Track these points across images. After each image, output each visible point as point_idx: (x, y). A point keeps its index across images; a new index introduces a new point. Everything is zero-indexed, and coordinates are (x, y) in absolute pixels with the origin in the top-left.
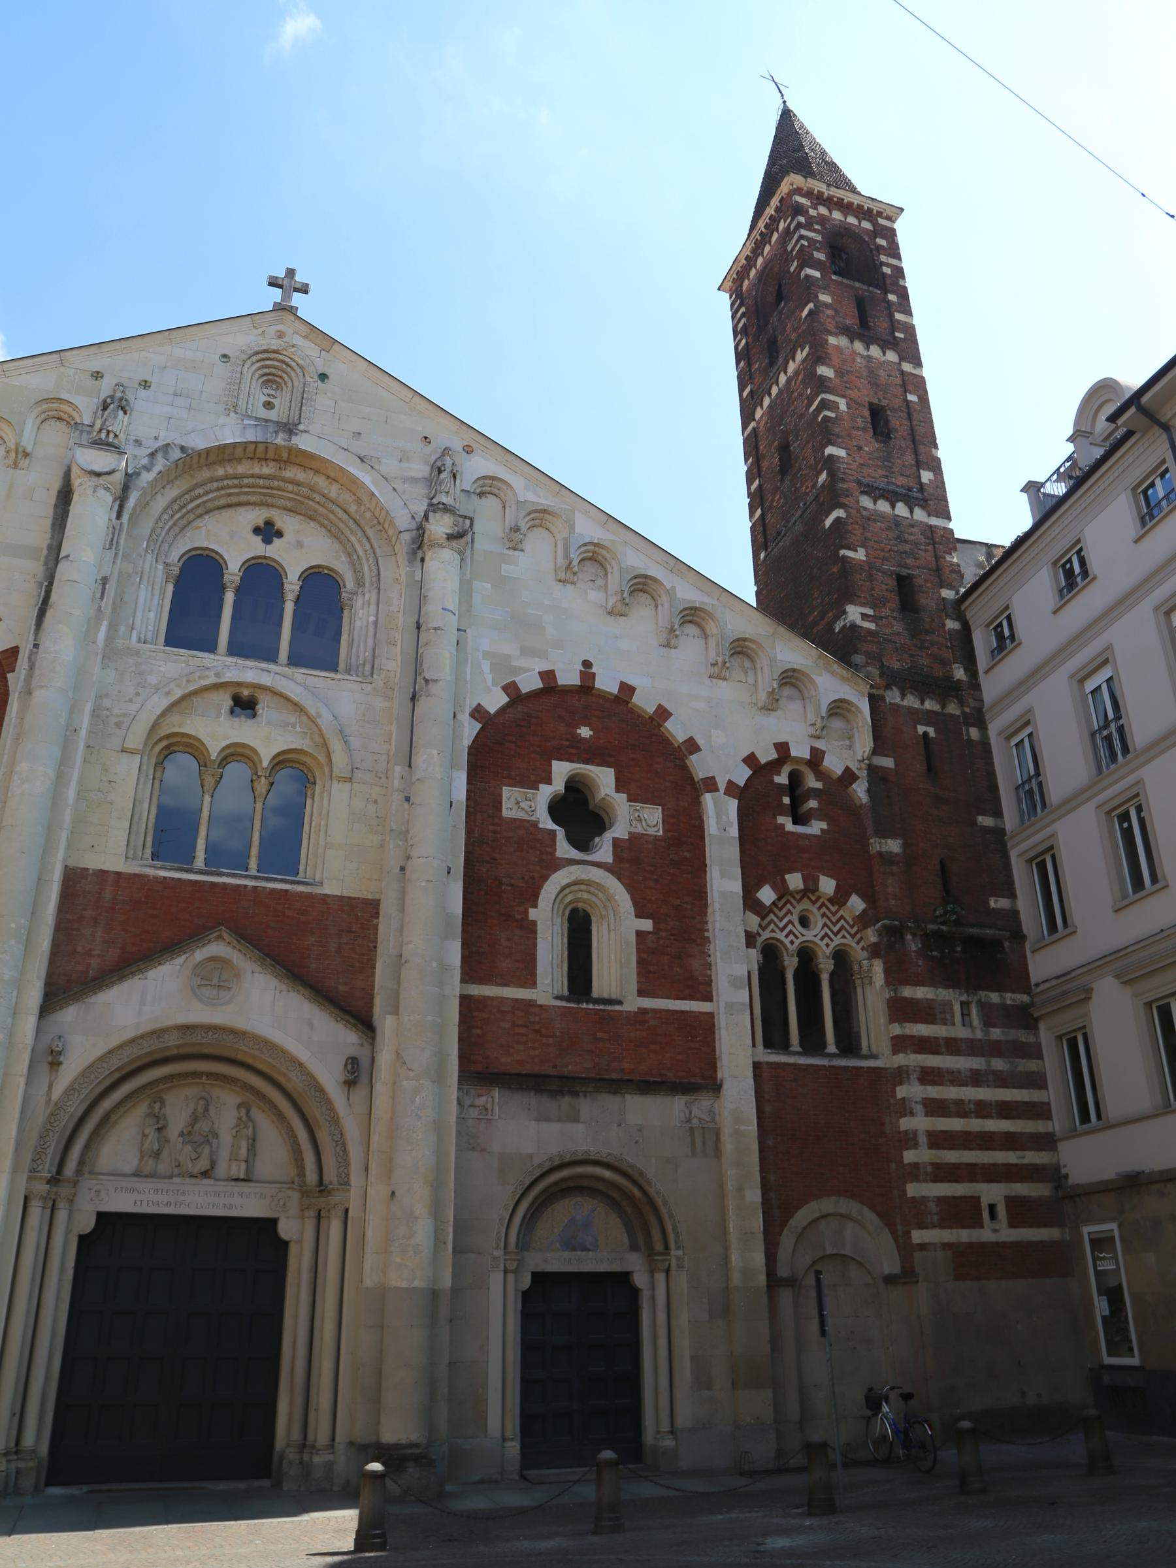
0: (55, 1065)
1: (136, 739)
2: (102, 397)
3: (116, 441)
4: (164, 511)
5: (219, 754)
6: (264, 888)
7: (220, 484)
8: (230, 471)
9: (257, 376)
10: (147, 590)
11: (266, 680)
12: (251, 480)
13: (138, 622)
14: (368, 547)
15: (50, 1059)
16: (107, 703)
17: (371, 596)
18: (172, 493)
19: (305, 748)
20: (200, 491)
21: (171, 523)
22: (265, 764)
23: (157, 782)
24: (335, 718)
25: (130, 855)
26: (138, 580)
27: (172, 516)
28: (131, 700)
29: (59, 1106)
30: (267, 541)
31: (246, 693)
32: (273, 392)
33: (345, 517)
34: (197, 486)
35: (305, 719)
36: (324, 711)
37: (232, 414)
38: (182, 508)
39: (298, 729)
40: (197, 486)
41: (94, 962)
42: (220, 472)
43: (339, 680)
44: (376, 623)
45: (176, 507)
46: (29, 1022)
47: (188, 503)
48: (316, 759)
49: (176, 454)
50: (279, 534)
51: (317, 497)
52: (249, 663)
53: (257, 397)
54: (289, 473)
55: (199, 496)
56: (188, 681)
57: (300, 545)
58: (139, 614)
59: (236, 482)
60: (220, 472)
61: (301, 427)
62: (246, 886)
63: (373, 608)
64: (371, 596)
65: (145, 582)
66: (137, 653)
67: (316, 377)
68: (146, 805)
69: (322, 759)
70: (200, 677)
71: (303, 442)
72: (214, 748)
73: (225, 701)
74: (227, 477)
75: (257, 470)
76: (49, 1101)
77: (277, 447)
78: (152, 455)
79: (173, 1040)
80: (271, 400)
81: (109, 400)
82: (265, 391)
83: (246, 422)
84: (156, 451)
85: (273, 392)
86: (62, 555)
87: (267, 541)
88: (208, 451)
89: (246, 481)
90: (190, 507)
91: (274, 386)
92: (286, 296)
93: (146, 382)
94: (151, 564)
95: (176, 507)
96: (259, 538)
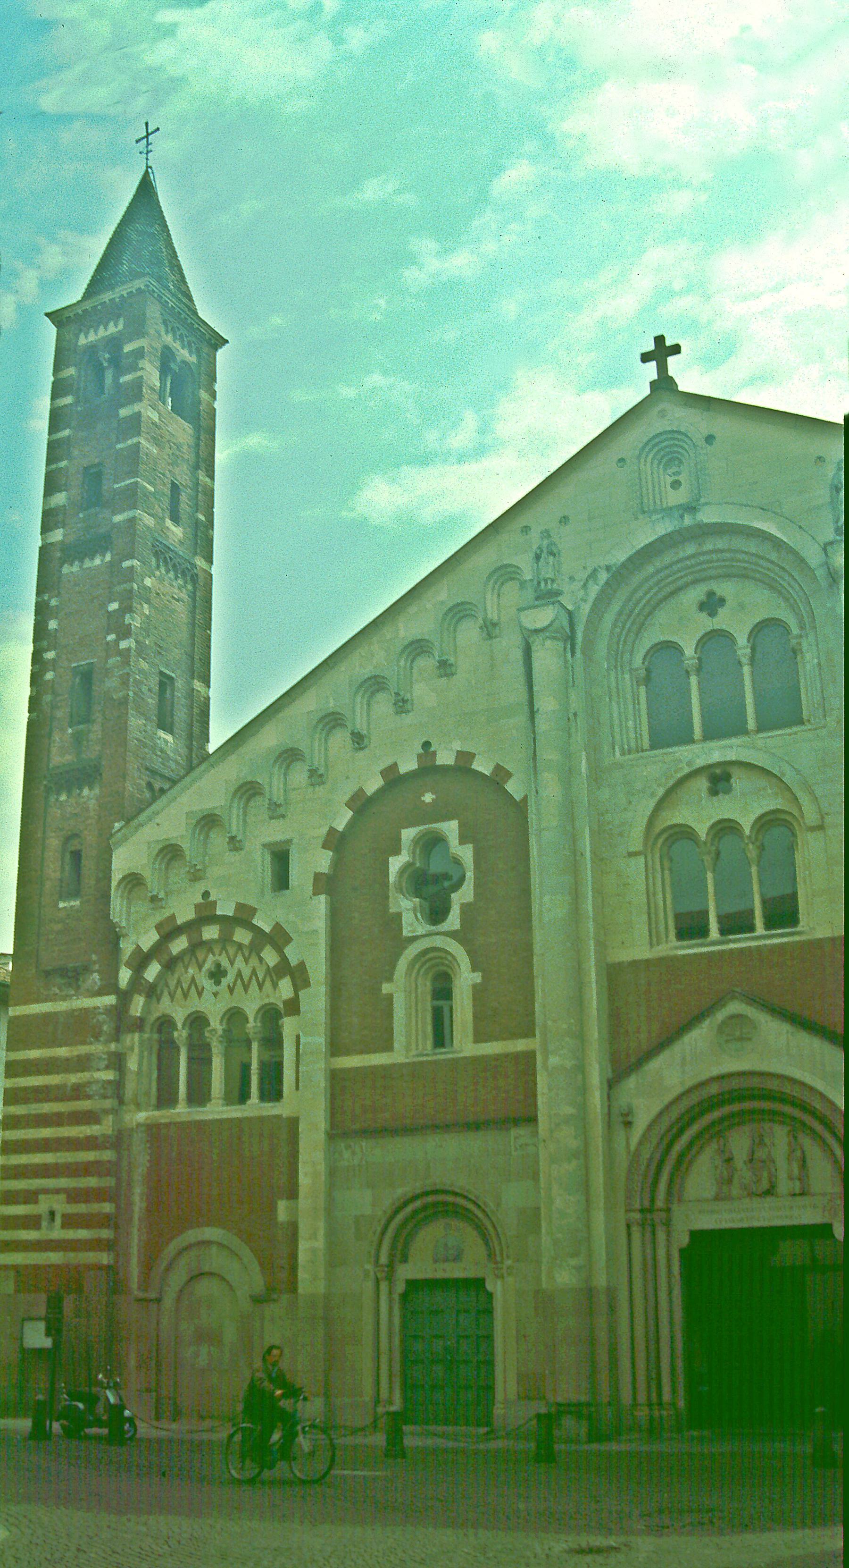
0: (628, 1124)
1: (636, 844)
2: (535, 547)
3: (555, 586)
4: (615, 625)
5: (707, 834)
6: (765, 945)
7: (655, 579)
8: (658, 564)
9: (656, 462)
10: (618, 703)
11: (731, 756)
12: (679, 565)
13: (617, 738)
14: (797, 588)
15: (621, 1119)
16: (608, 817)
17: (811, 638)
18: (616, 607)
19: (779, 807)
20: (640, 593)
21: (624, 633)
22: (747, 832)
23: (667, 872)
24: (798, 772)
25: (655, 939)
26: (608, 700)
27: (623, 627)
28: (625, 809)
29: (637, 1153)
30: (712, 614)
31: (718, 771)
32: (675, 469)
33: (771, 566)
34: (635, 591)
35: (774, 780)
36: (787, 769)
37: (641, 517)
38: (629, 616)
39: (770, 791)
40: (635, 591)
41: (643, 1036)
42: (651, 569)
43: (796, 733)
44: (819, 664)
45: (624, 617)
46: (596, 1099)
47: (634, 609)
48: (791, 814)
49: (603, 576)
50: (722, 601)
51: (739, 556)
52: (713, 744)
53: (662, 484)
54: (708, 546)
55: (641, 598)
56: (667, 779)
57: (741, 606)
58: (617, 729)
59: (667, 572)
60: (651, 569)
61: (702, 500)
62: (750, 947)
63: (814, 647)
64: (811, 638)
65: (615, 698)
66: (621, 766)
67: (704, 444)
68: (660, 896)
69: (796, 812)
70: (676, 772)
71: (708, 516)
72: (702, 830)
73: (702, 784)
74: (658, 572)
75: (681, 555)
76: (629, 1153)
77: (688, 529)
78: (585, 586)
79: (714, 1089)
80: (676, 478)
81: (538, 552)
82: (670, 471)
83: (654, 517)
84: (587, 580)
85: (675, 469)
86: (535, 710)
87: (712, 614)
88: (630, 559)
89: (675, 568)
90: (637, 611)
91: (677, 463)
92: (662, 368)
93: (564, 517)
94: (617, 678)
95: (624, 617)
96: (704, 615)
